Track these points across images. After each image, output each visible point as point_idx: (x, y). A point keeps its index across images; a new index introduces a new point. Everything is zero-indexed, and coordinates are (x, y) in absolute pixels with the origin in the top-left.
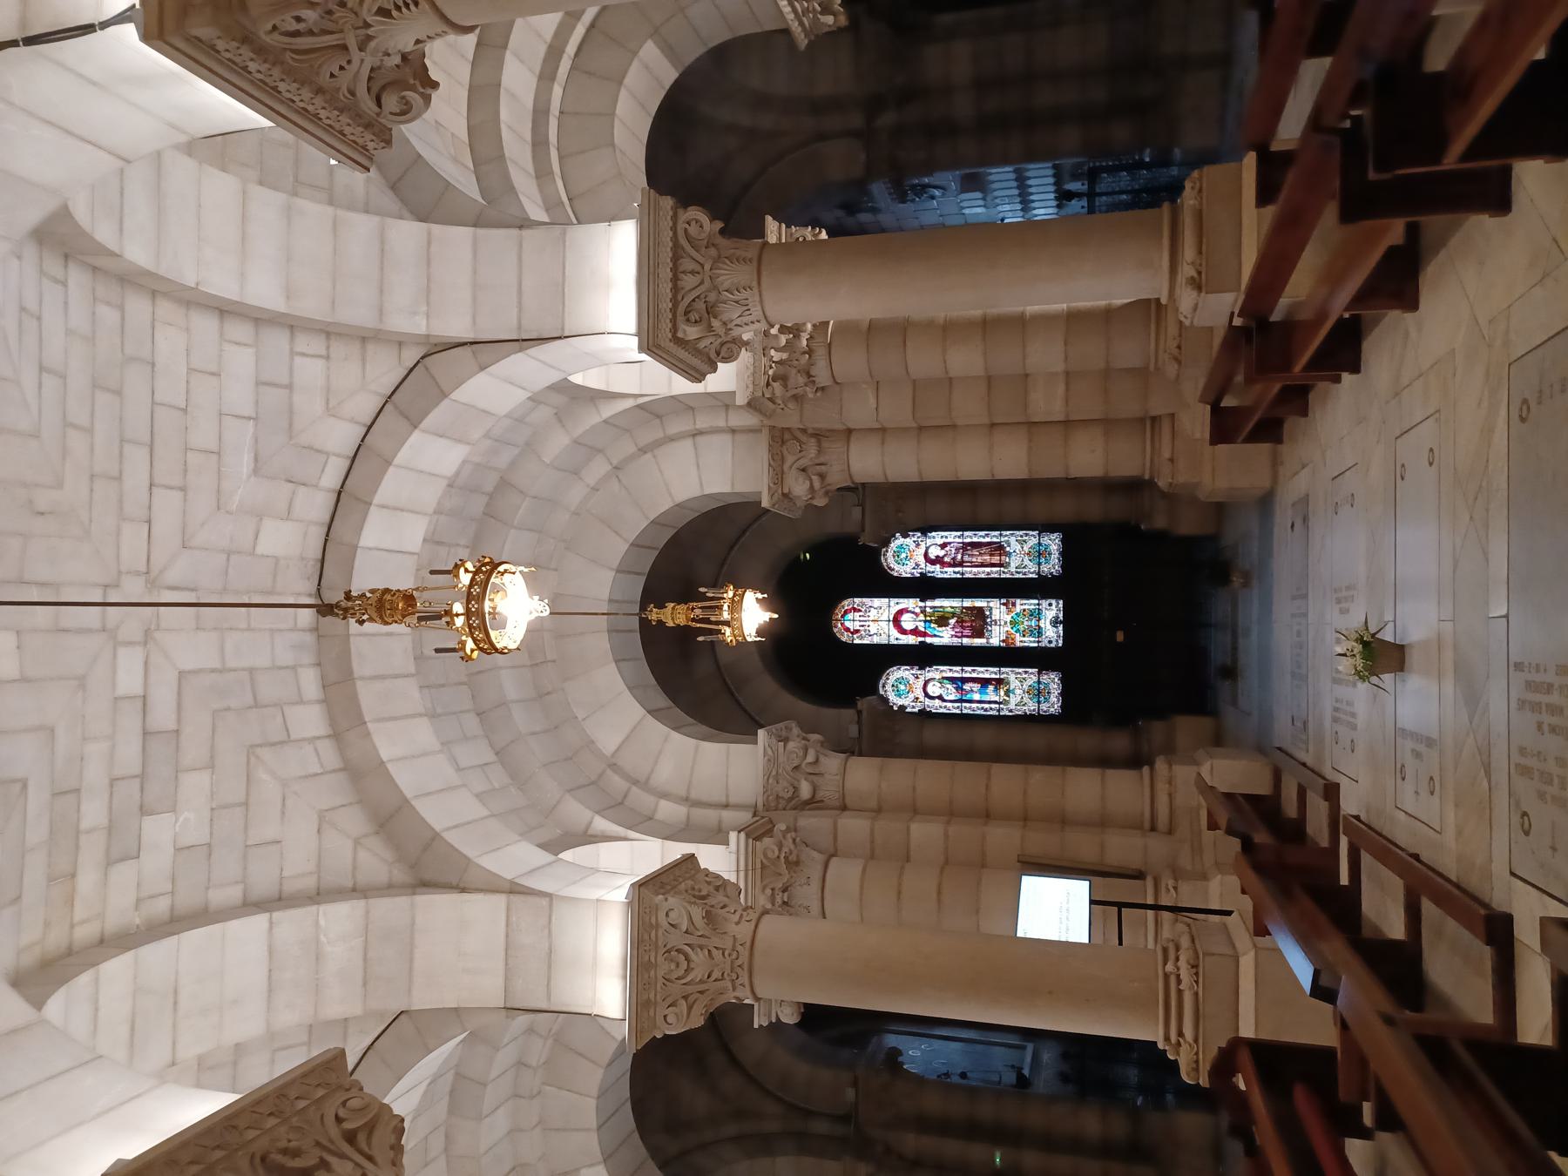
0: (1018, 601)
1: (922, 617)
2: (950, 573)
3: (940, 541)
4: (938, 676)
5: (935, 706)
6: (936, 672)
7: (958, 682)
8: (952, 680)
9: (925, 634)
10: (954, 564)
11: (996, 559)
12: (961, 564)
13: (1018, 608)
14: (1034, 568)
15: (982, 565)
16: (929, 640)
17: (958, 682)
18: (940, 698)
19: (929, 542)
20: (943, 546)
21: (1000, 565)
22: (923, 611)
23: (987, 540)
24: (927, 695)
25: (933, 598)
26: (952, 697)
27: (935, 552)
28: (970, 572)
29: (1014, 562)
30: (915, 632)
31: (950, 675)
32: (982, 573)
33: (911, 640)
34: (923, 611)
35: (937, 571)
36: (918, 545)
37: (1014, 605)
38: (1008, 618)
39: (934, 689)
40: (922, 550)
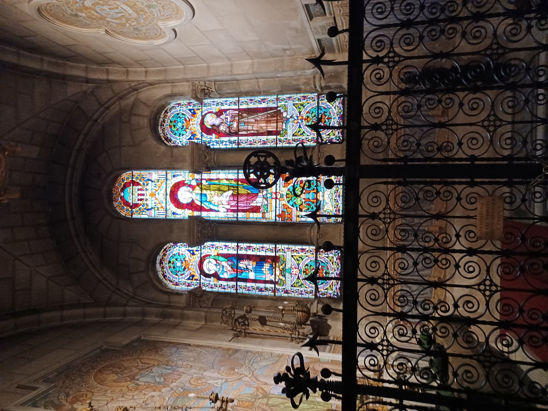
9: (201, 209)
16: (204, 214)
30: (191, 206)
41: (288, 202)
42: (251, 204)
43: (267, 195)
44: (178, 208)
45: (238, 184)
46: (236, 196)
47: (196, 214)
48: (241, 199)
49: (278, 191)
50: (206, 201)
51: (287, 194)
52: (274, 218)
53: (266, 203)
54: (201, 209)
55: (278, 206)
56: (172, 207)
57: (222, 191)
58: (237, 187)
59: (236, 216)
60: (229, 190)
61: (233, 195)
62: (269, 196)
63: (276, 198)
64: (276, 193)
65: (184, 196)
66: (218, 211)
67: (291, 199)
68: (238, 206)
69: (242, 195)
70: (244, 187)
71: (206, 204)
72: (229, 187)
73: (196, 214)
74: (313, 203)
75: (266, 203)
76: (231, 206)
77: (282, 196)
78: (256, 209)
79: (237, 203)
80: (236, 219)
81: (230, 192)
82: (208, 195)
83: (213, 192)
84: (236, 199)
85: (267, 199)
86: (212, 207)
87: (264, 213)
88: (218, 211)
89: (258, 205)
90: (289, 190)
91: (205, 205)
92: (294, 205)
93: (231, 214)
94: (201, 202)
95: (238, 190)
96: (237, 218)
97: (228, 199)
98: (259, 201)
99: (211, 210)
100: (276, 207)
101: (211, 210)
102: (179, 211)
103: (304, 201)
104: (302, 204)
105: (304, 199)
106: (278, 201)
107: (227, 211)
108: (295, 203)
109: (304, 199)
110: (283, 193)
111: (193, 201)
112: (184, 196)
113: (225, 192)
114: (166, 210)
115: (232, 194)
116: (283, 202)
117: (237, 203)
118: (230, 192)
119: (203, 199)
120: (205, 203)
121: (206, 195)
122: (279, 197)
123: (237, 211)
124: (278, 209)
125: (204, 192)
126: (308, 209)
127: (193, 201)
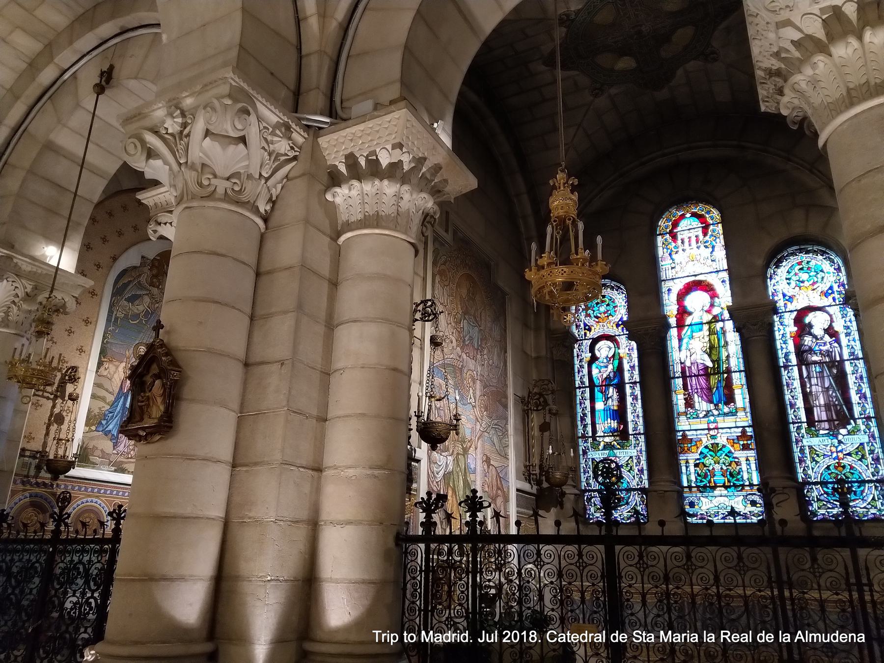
0: (752, 454)
1: (708, 317)
2: (785, 347)
3: (838, 326)
4: (623, 351)
5: (582, 353)
6: (629, 350)
7: (617, 380)
8: (620, 370)
9: (680, 325)
10: (800, 352)
11: (820, 414)
12: (802, 361)
13: (741, 455)
14: (814, 477)
15: (806, 396)
16: (674, 332)
17: (617, 380)
18: (594, 359)
19: (835, 310)
20: (830, 331)
21: (811, 421)
22: (716, 319)
23: (855, 398)
24: (595, 341)
25: (738, 329)
26: (595, 372)
27: (819, 322)
28: (792, 377)
29: (820, 442)
30: (683, 312)
31: (626, 367)
32: (794, 395)
33: (671, 308)
34: (716, 319)
35: (785, 328)
36: (826, 294)
37: (745, 447)
38: (722, 440)
39: (604, 349)
40: (817, 301)
41: (706, 447)
42: (696, 395)
43: (713, 415)
44: (678, 295)
45: (724, 373)
46: (706, 373)
47: (673, 321)
48: (702, 380)
49: (720, 431)
50: (692, 332)
51: (717, 444)
52: (680, 428)
53: (701, 415)
54: (680, 325)
55: (699, 432)
56: (677, 286)
57: (710, 351)
58: (719, 373)
59: (677, 375)
60: (713, 361)
61: (706, 368)
62: (712, 418)
63: (709, 429)
64: (717, 428)
65: (697, 301)
66: (680, 350)
67: (710, 450)
68: (691, 376)
69: (708, 380)
70: (719, 381)
71: (689, 333)
72: (717, 361)
73: (673, 321)
74: (710, 482)
75: (701, 415)
76: (690, 368)
77: (713, 437)
78: (689, 403)
79: (695, 376)
80: (672, 375)
81: (710, 364)
82: (701, 333)
83: (707, 339)
84: (701, 372)
85: (706, 416)
86: (685, 341)
87: (686, 413)
88: (680, 350)
89: (697, 406)
90: (724, 446)
91: (686, 331)
92: (702, 456)
93: (678, 369)
94: (691, 325)
95: (714, 374)
96: (674, 378)
97: (699, 361)
98: (701, 405)
99: (680, 339)
100: (696, 430)
101: (680, 339)
102: (673, 297)
103: (711, 468)
104: (705, 466)
105: (713, 469)
106: (706, 432)
107: (681, 363)
108: (705, 456)
109: (713, 469)
110: (719, 439)
111: (690, 314)
112: (697, 301)
113: (710, 356)
114: (673, 279)
115: (708, 367)
116: (704, 440)
117: (695, 376)
118: (710, 364)
119: (694, 327)
120: (690, 330)
121: (701, 330)
122: (712, 433)
123: (684, 376)
124: (694, 432)
125: (706, 327)
126: (699, 475)
127: (690, 314)
